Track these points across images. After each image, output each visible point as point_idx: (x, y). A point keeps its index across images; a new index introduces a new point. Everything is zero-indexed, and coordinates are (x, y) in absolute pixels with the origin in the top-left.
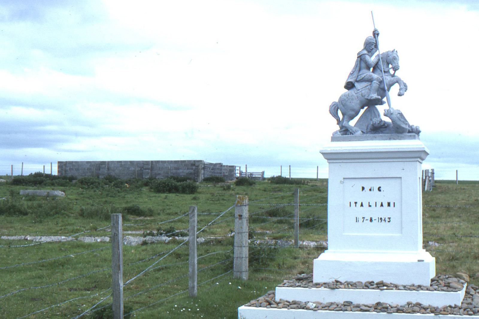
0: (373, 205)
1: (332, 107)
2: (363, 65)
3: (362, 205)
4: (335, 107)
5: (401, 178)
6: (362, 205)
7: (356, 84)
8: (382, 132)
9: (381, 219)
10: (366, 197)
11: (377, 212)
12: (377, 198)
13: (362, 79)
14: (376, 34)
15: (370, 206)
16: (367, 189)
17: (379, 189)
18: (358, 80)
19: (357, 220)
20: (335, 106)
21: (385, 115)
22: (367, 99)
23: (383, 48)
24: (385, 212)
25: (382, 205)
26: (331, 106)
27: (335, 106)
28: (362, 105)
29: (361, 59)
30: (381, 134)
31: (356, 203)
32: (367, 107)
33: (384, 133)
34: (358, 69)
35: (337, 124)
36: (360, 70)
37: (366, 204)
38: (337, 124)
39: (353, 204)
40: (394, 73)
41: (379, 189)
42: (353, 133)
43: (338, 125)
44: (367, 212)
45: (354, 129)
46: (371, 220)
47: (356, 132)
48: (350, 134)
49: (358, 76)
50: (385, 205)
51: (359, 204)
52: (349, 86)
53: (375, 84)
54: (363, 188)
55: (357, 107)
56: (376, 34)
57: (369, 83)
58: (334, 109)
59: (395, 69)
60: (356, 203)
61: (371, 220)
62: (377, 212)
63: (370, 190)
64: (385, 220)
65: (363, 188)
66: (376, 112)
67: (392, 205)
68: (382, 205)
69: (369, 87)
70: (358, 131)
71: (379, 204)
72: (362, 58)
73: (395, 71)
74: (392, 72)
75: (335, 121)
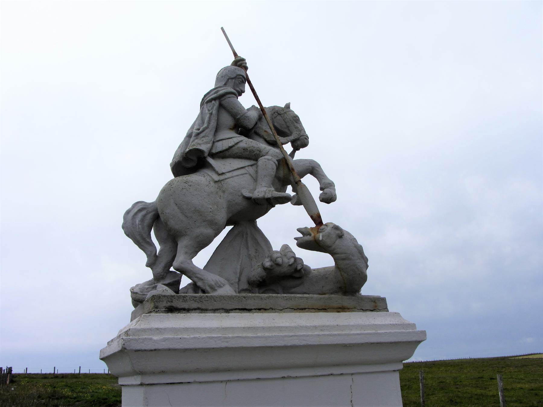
1: (136, 214)
2: (227, 120)
4: (144, 216)
7: (210, 160)
13: (227, 150)
18: (214, 151)
20: (143, 213)
22: (249, 199)
26: (132, 214)
27: (143, 213)
28: (230, 215)
29: (221, 106)
30: (284, 293)
32: (231, 227)
33: (292, 293)
34: (213, 124)
35: (148, 265)
36: (217, 130)
38: (148, 265)
40: (293, 154)
42: (208, 289)
43: (149, 269)
45: (212, 278)
47: (220, 287)
49: (214, 142)
55: (222, 216)
58: (142, 220)
66: (260, 240)
69: (251, 170)
70: (224, 285)
72: (226, 101)
73: (296, 148)
74: (288, 148)
75: (142, 257)
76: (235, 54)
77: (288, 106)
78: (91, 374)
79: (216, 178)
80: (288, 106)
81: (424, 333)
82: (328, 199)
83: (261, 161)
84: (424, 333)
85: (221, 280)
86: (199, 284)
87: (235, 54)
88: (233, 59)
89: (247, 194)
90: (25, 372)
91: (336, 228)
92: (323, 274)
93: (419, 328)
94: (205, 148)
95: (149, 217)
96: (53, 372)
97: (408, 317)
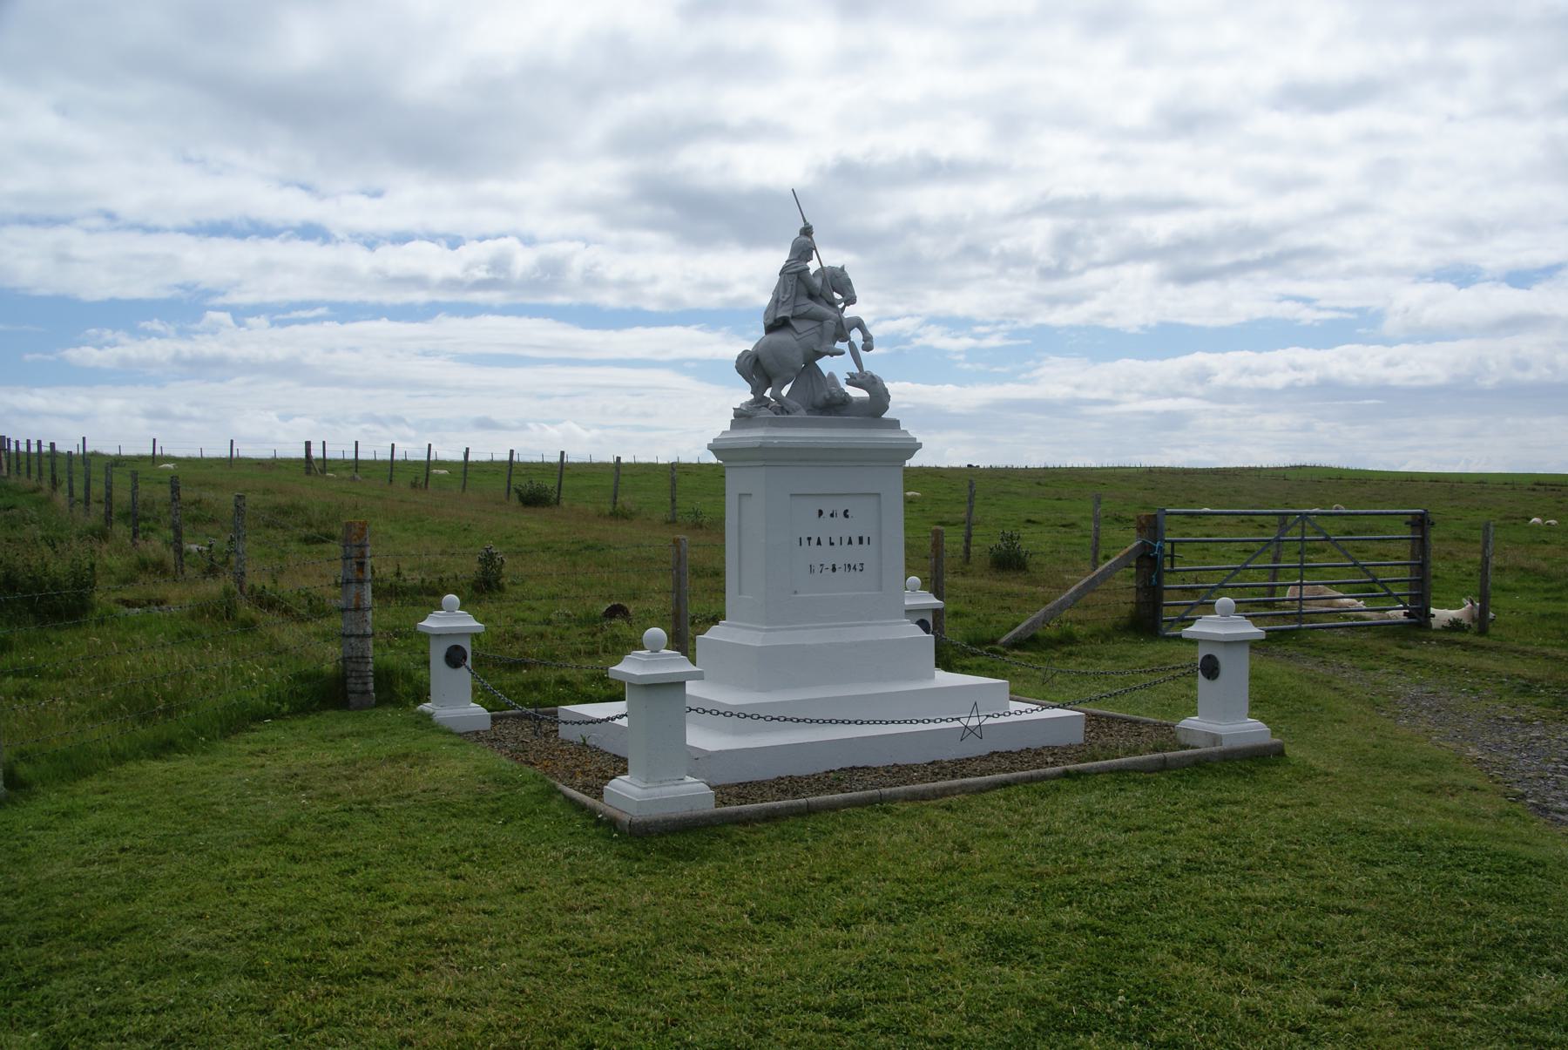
0: (836, 541)
2: (803, 289)
3: (819, 543)
5: (879, 495)
6: (819, 543)
7: (793, 323)
8: (837, 413)
9: (849, 565)
10: (827, 528)
11: (843, 555)
12: (840, 528)
14: (807, 231)
15: (832, 544)
16: (826, 513)
17: (846, 514)
19: (812, 570)
21: (849, 383)
23: (827, 257)
24: (855, 554)
25: (850, 542)
26: (743, 359)
31: (809, 539)
34: (794, 294)
37: (825, 541)
39: (805, 541)
41: (846, 514)
44: (826, 555)
45: (794, 404)
46: (834, 569)
48: (783, 414)
50: (855, 541)
51: (814, 541)
52: (775, 326)
53: (830, 325)
54: (821, 513)
56: (807, 231)
57: (818, 323)
59: (851, 300)
60: (809, 539)
61: (834, 569)
62: (843, 555)
63: (832, 515)
64: (855, 568)
65: (821, 513)
67: (865, 541)
68: (850, 542)
69: (818, 329)
71: (845, 541)
76: (805, 221)
77: (843, 269)
78: (497, 462)
79: (798, 337)
80: (843, 269)
81: (921, 444)
82: (868, 348)
83: (827, 323)
84: (921, 444)
85: (796, 404)
86: (786, 407)
87: (805, 221)
88: (802, 225)
89: (816, 349)
90: (81, 451)
91: (873, 377)
92: (861, 402)
93: (918, 441)
94: (788, 314)
95: (753, 361)
96: (150, 452)
97: (912, 433)
